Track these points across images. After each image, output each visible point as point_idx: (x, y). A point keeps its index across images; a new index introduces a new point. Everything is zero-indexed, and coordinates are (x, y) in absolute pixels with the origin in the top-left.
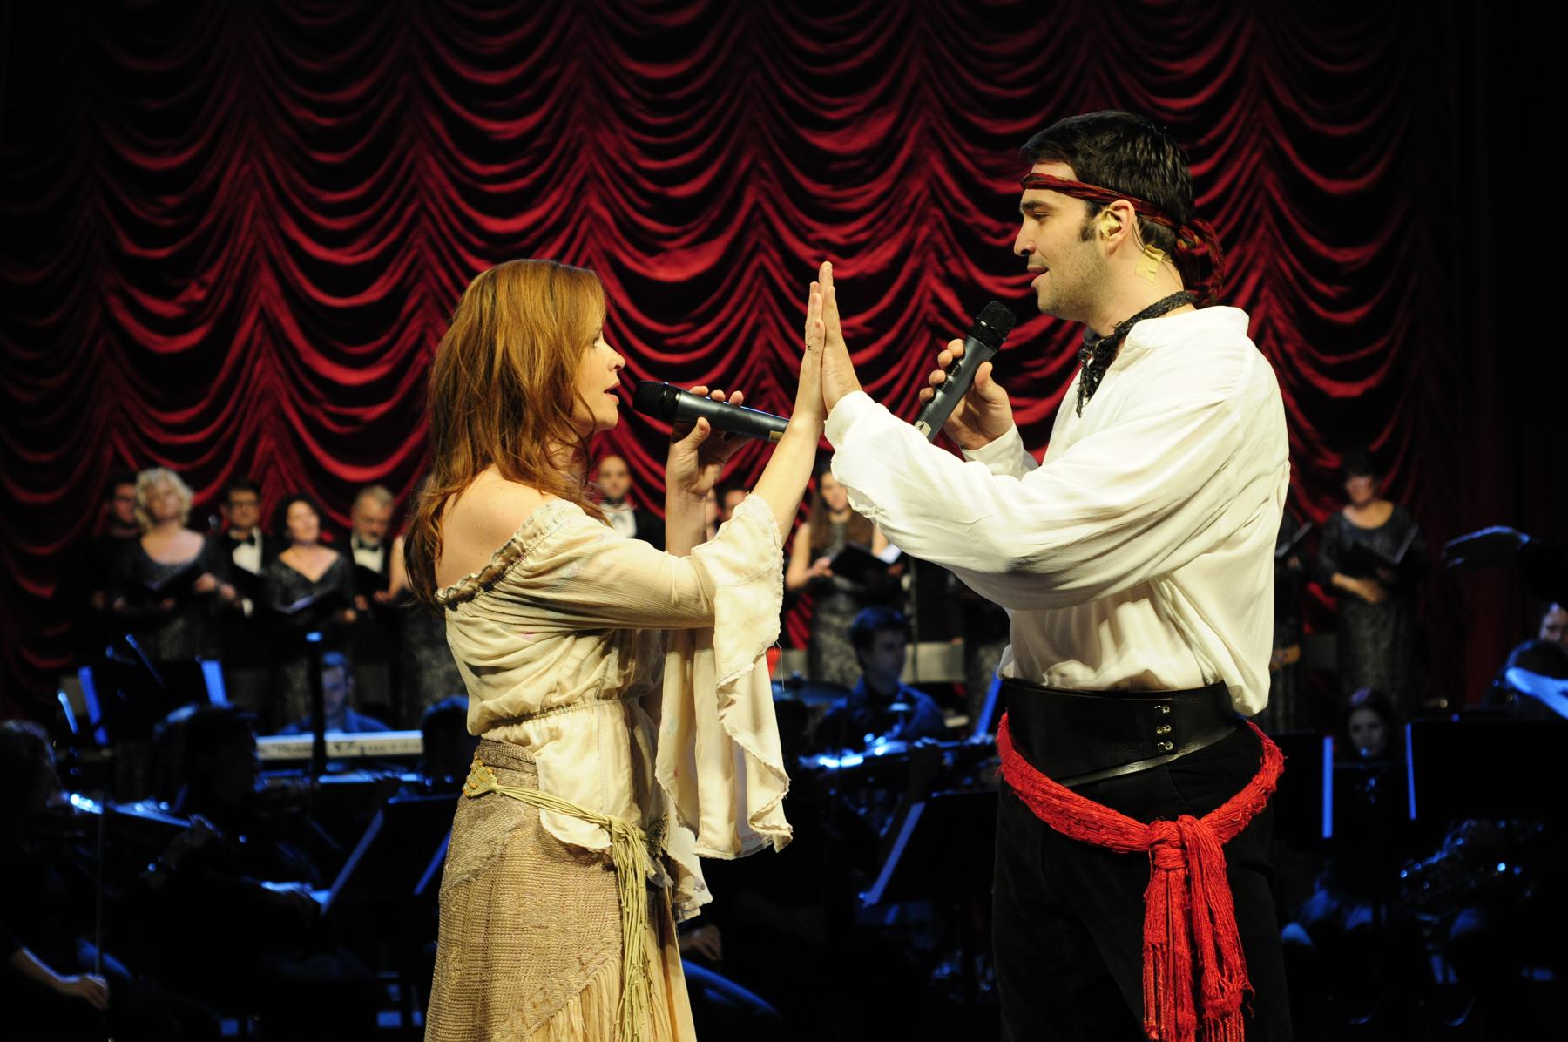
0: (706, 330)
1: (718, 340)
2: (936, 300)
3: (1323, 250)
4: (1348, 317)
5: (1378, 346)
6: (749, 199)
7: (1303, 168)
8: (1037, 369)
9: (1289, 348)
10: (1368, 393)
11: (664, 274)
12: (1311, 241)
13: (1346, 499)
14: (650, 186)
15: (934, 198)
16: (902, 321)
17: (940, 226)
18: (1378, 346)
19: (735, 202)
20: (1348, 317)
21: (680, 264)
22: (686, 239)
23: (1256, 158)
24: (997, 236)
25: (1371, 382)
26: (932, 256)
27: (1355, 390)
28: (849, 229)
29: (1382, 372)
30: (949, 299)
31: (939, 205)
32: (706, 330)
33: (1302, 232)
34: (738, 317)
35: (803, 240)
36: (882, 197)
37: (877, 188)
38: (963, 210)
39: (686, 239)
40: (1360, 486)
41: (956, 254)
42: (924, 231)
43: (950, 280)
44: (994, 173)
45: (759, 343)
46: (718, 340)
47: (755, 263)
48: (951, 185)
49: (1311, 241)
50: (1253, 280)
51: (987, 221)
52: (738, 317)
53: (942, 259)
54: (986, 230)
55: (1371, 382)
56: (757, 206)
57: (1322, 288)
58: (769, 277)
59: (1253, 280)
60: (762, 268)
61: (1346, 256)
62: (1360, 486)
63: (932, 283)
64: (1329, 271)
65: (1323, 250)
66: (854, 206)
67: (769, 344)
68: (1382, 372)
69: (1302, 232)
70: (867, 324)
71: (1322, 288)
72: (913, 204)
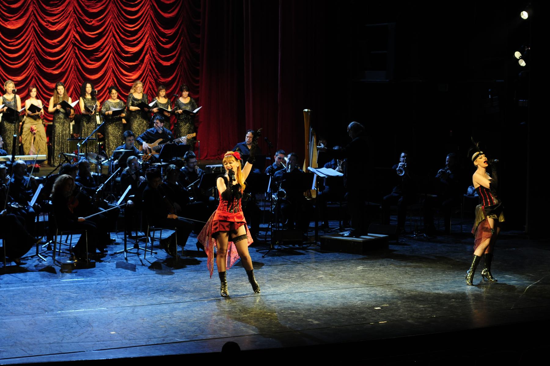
0: (19, 41)
1: (22, 44)
2: (74, 37)
3: (163, 30)
4: (168, 46)
5: (174, 53)
6: (31, 9)
7: (159, 10)
8: (97, 55)
9: (154, 53)
10: (171, 65)
11: (9, 27)
12: (160, 28)
13: (181, 96)
14: (7, 5)
15: (74, 11)
16: (66, 42)
17: (76, 19)
18: (174, 53)
19: (27, 9)
20: (168, 46)
21: (13, 24)
22: (15, 18)
23: (148, 7)
24: (89, 22)
25: (172, 62)
26: (73, 26)
27: (168, 64)
28: (55, 18)
29: (174, 59)
30: (78, 37)
31: (76, 14)
32: (19, 41)
33: (158, 26)
34: (27, 38)
35: (45, 22)
36: (62, 11)
37: (60, 8)
38: (81, 15)
39: (15, 18)
40: (185, 93)
41: (79, 26)
42: (72, 20)
43: (77, 32)
44: (88, 6)
45: (32, 45)
46: (22, 44)
47: (31, 25)
48: (79, 9)
49: (160, 28)
50: (147, 36)
51: (87, 19)
52: (27, 38)
53: (76, 27)
54: (87, 21)
55: (172, 62)
56: (32, 11)
57: (162, 39)
58: (35, 29)
59: (147, 36)
60: (33, 26)
61: (169, 32)
62: (185, 93)
63: (73, 33)
64: (164, 35)
65: (163, 30)
66: (56, 13)
67: (34, 45)
68: (174, 59)
69: (158, 26)
70: (58, 42)
71: (162, 39)
72: (70, 13)
